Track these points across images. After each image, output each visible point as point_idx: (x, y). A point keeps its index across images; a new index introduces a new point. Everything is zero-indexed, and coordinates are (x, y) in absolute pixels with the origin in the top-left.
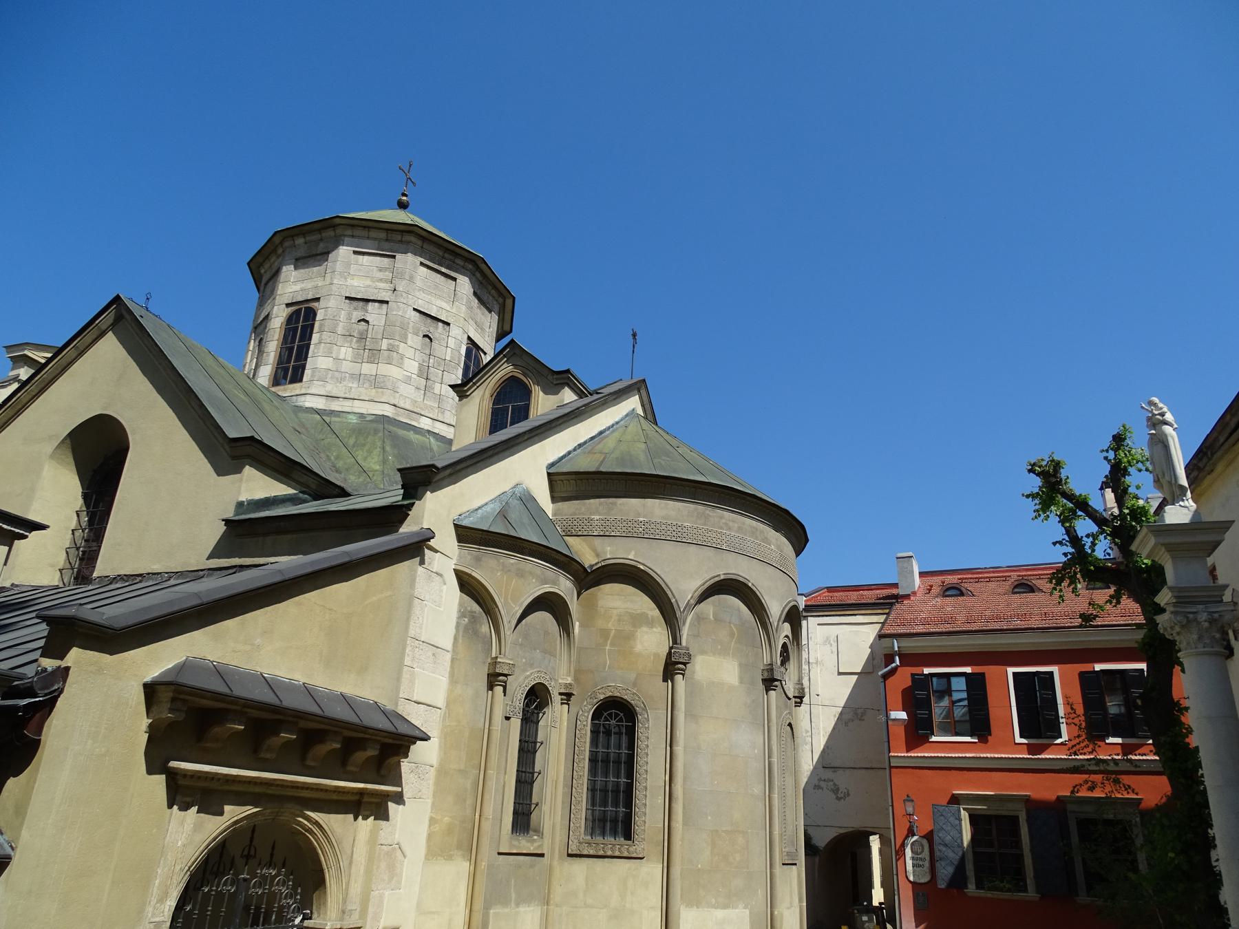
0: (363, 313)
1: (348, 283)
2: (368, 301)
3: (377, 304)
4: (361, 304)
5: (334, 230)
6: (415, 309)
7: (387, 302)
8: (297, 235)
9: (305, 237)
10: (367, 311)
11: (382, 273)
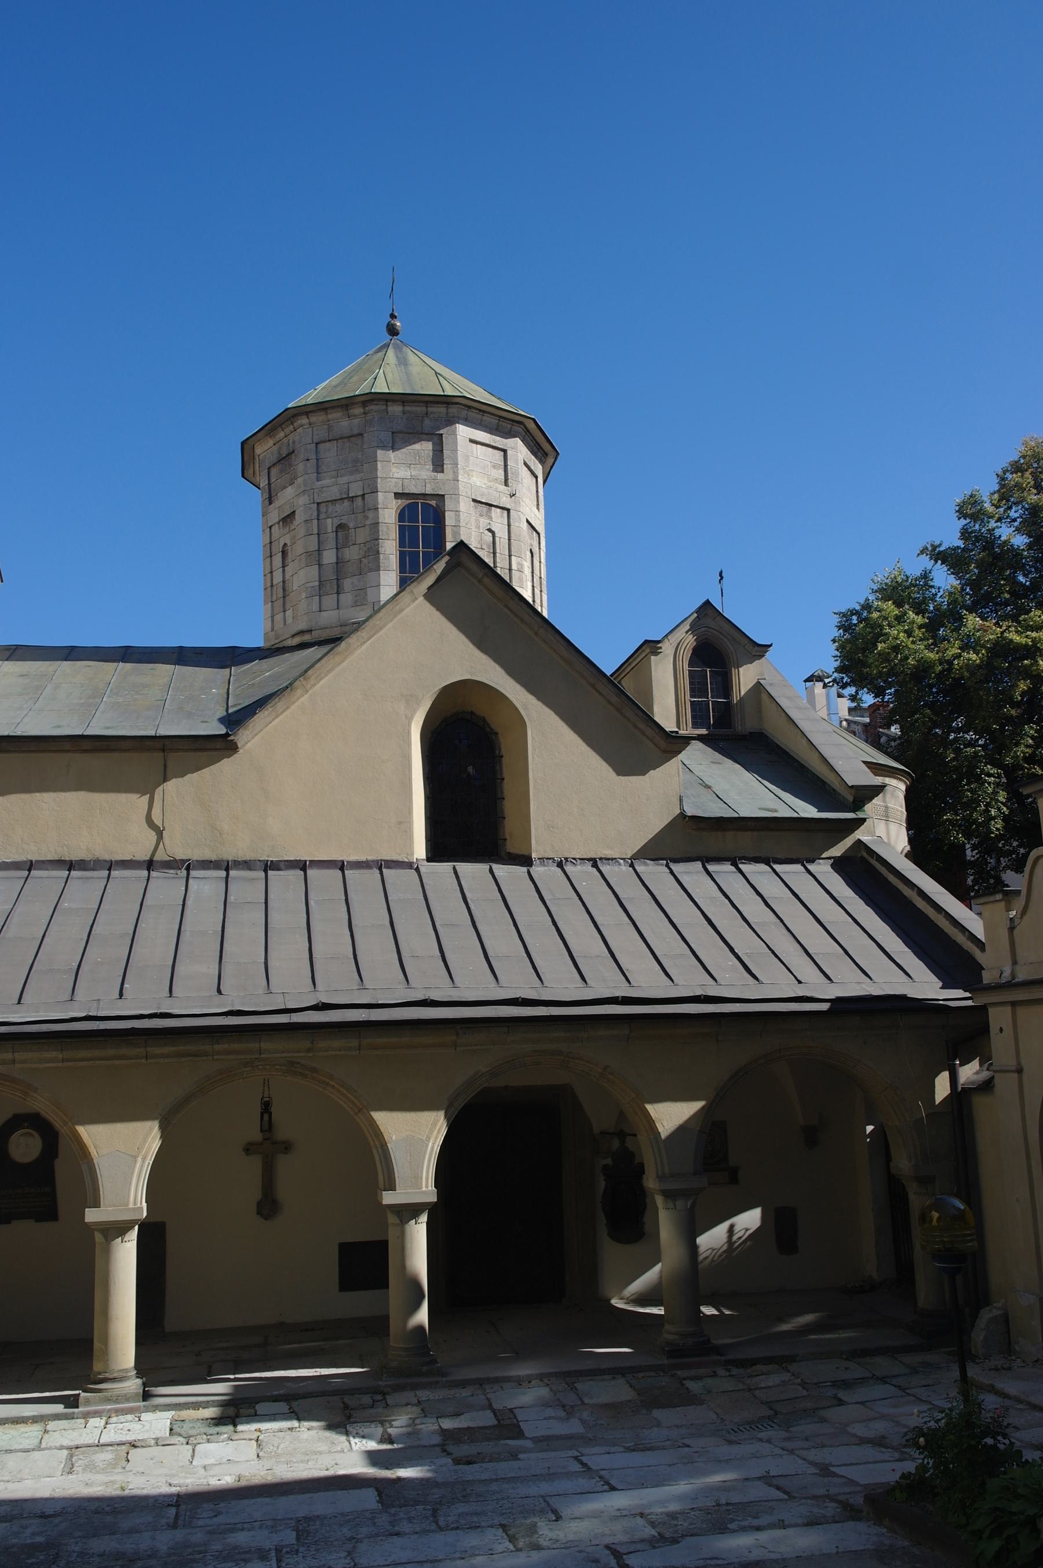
0: (488, 521)
1: (471, 481)
2: (491, 505)
3: (498, 510)
4: (485, 508)
5: (447, 408)
6: (528, 521)
7: (508, 510)
8: (393, 401)
9: (404, 406)
10: (491, 518)
11: (495, 470)
